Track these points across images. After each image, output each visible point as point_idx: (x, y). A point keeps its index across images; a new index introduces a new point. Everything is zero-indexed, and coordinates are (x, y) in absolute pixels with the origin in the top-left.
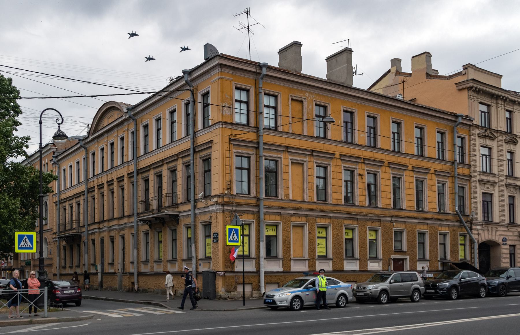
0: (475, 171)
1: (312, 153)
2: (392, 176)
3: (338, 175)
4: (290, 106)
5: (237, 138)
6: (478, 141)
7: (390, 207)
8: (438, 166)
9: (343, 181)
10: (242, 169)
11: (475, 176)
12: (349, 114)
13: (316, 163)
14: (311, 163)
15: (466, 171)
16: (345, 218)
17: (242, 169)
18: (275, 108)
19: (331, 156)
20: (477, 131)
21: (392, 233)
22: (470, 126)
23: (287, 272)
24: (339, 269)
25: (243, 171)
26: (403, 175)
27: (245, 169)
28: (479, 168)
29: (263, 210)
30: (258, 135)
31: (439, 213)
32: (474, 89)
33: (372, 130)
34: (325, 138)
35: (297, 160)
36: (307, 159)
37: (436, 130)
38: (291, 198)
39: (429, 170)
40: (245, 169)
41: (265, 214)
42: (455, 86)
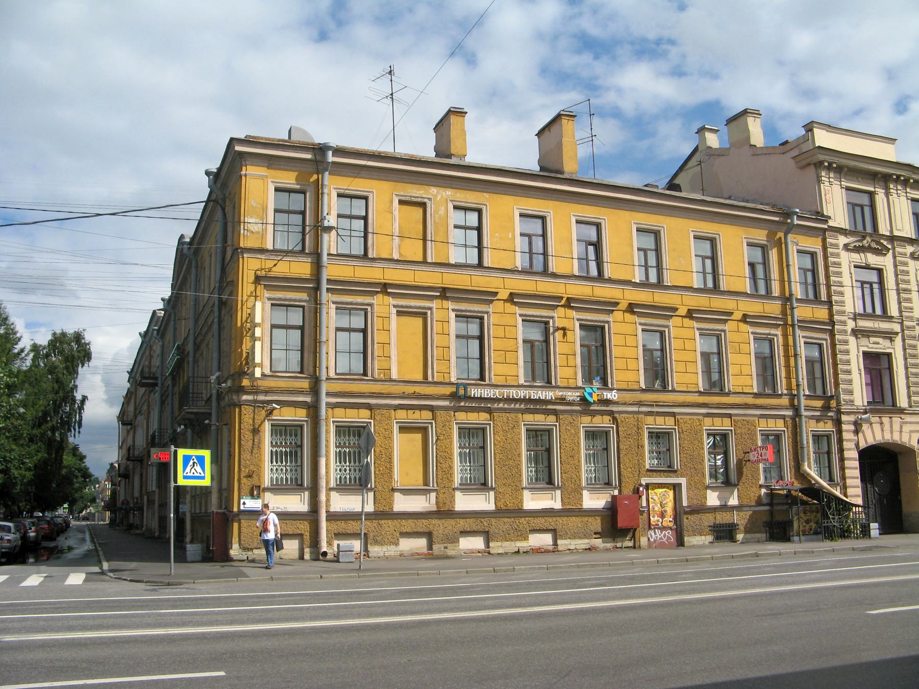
0: (842, 313)
1: (445, 293)
2: (640, 328)
3: (509, 330)
4: (396, 213)
5: (272, 274)
6: (846, 260)
7: (636, 387)
8: (754, 307)
9: (520, 341)
10: (468, 337)
11: (844, 323)
12: (540, 221)
13: (521, 315)
14: (445, 315)
15: (821, 313)
16: (523, 412)
17: (468, 337)
18: (479, 229)
19: (488, 296)
20: (842, 240)
21: (577, 433)
22: (825, 230)
23: (383, 514)
24: (511, 506)
25: (291, 331)
26: (668, 327)
27: (473, 337)
28: (849, 308)
29: (324, 400)
30: (317, 266)
31: (425, 381)
32: (826, 164)
33: (591, 248)
34: (480, 265)
35: (410, 307)
36: (435, 304)
37: (745, 242)
38: (394, 376)
39: (676, 309)
40: (473, 337)
41: (328, 404)
42: (792, 161)
